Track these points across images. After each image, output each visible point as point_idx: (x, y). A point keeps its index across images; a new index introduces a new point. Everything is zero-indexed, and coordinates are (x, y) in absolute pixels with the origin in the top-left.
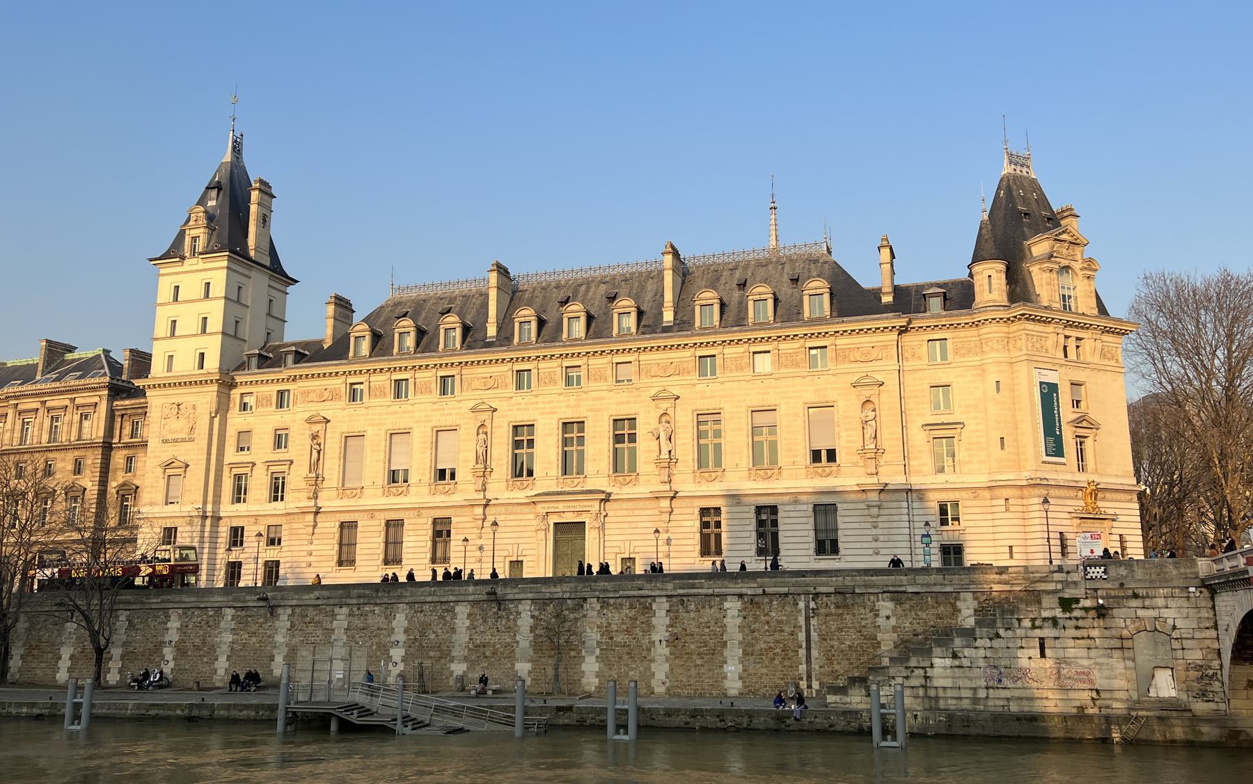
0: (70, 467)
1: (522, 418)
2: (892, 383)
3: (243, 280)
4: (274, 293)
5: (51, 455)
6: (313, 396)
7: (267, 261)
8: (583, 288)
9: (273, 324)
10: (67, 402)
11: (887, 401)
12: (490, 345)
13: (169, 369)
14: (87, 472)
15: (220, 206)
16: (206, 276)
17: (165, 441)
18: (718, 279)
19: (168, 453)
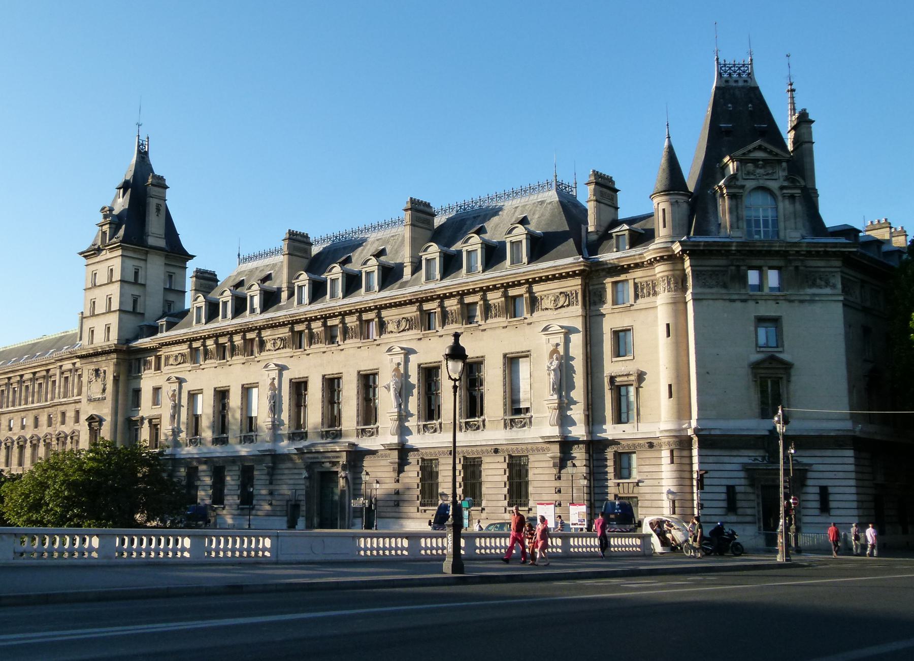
3: (141, 264)
4: (172, 270)
6: (171, 361)
9: (171, 297)
16: (110, 263)
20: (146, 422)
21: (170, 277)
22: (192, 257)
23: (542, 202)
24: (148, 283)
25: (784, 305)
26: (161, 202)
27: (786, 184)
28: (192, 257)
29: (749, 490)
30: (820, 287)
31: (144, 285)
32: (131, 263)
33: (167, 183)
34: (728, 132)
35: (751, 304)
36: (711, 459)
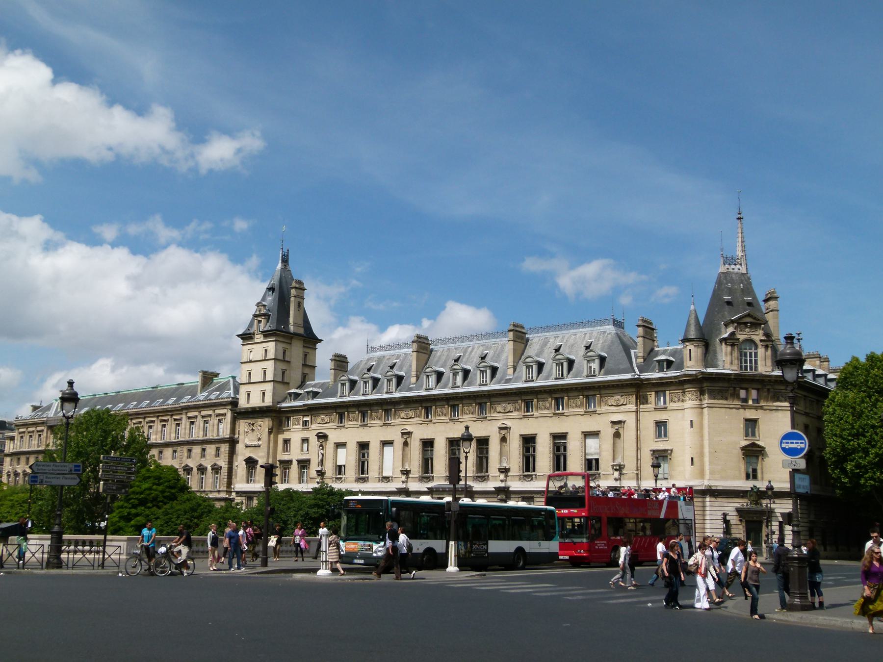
0: (214, 452)
1: (427, 436)
2: (630, 420)
4: (307, 350)
5: (204, 446)
7: (301, 331)
8: (470, 349)
9: (307, 371)
10: (210, 412)
11: (629, 433)
12: (410, 389)
13: (248, 402)
14: (222, 456)
15: (274, 300)
17: (247, 446)
18: (546, 345)
19: (249, 453)
20: (295, 463)
21: (306, 355)
22: (321, 341)
23: (604, 332)
24: (292, 360)
25: (760, 411)
26: (300, 300)
27: (764, 338)
28: (321, 341)
29: (739, 523)
30: (781, 401)
31: (289, 362)
32: (281, 346)
33: (305, 286)
34: (729, 303)
35: (742, 410)
36: (717, 504)
